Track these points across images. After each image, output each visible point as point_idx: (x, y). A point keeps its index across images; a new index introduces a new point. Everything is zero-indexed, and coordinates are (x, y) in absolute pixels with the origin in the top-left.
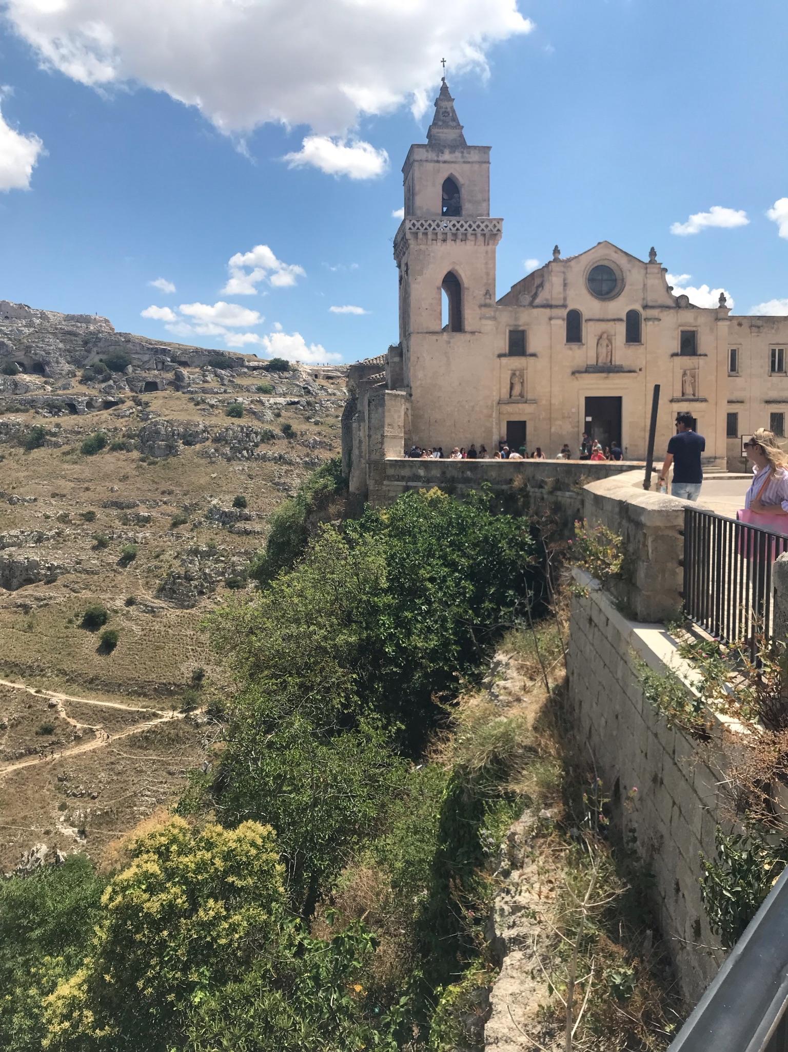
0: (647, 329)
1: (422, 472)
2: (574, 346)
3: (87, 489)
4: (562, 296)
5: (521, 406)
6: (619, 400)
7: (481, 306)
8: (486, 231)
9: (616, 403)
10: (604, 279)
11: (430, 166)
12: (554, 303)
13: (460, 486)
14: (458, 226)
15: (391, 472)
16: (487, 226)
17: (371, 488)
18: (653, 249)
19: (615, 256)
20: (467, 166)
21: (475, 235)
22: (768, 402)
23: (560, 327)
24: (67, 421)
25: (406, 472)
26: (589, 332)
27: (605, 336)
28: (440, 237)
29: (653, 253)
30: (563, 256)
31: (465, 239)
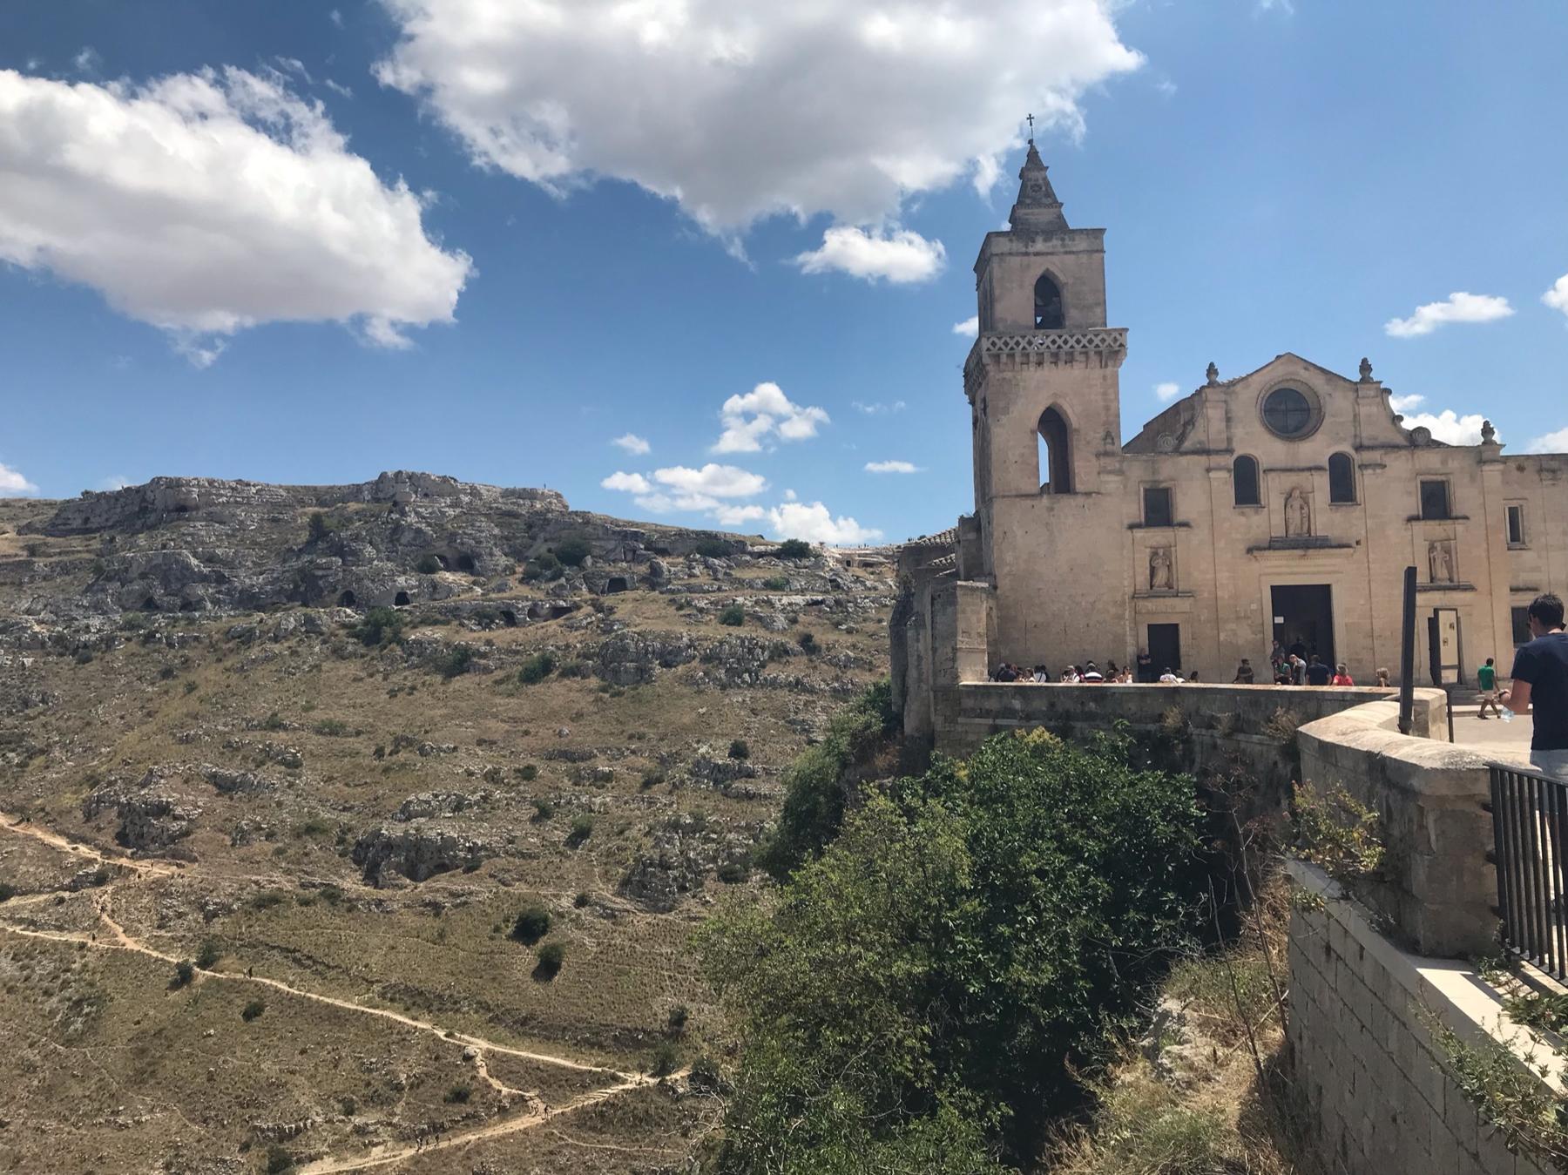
0: (1365, 482)
1: (1017, 704)
2: (1249, 510)
3: (526, 733)
4: (1224, 436)
5: (1170, 601)
6: (1326, 590)
7: (1098, 455)
8: (1103, 347)
9: (1320, 596)
10: (1291, 406)
11: (1015, 261)
12: (1212, 447)
13: (1078, 725)
14: (1060, 342)
15: (969, 703)
16: (1103, 340)
17: (938, 728)
18: (1364, 361)
19: (1304, 375)
21: (1086, 353)
23: (1224, 483)
24: (502, 635)
25: (992, 704)
26: (1272, 489)
27: (1297, 493)
28: (1033, 358)
29: (1365, 367)
30: (1222, 378)
31: (1070, 359)
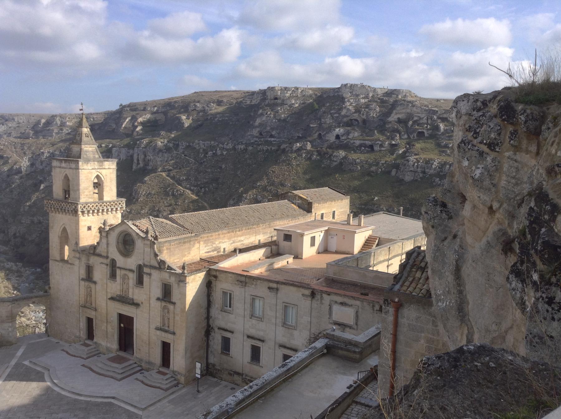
0: (146, 279)
4: (106, 250)
11: (58, 170)
20: (71, 170)
22: (249, 337)
